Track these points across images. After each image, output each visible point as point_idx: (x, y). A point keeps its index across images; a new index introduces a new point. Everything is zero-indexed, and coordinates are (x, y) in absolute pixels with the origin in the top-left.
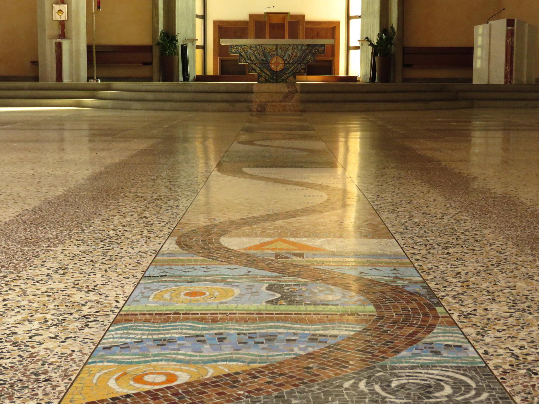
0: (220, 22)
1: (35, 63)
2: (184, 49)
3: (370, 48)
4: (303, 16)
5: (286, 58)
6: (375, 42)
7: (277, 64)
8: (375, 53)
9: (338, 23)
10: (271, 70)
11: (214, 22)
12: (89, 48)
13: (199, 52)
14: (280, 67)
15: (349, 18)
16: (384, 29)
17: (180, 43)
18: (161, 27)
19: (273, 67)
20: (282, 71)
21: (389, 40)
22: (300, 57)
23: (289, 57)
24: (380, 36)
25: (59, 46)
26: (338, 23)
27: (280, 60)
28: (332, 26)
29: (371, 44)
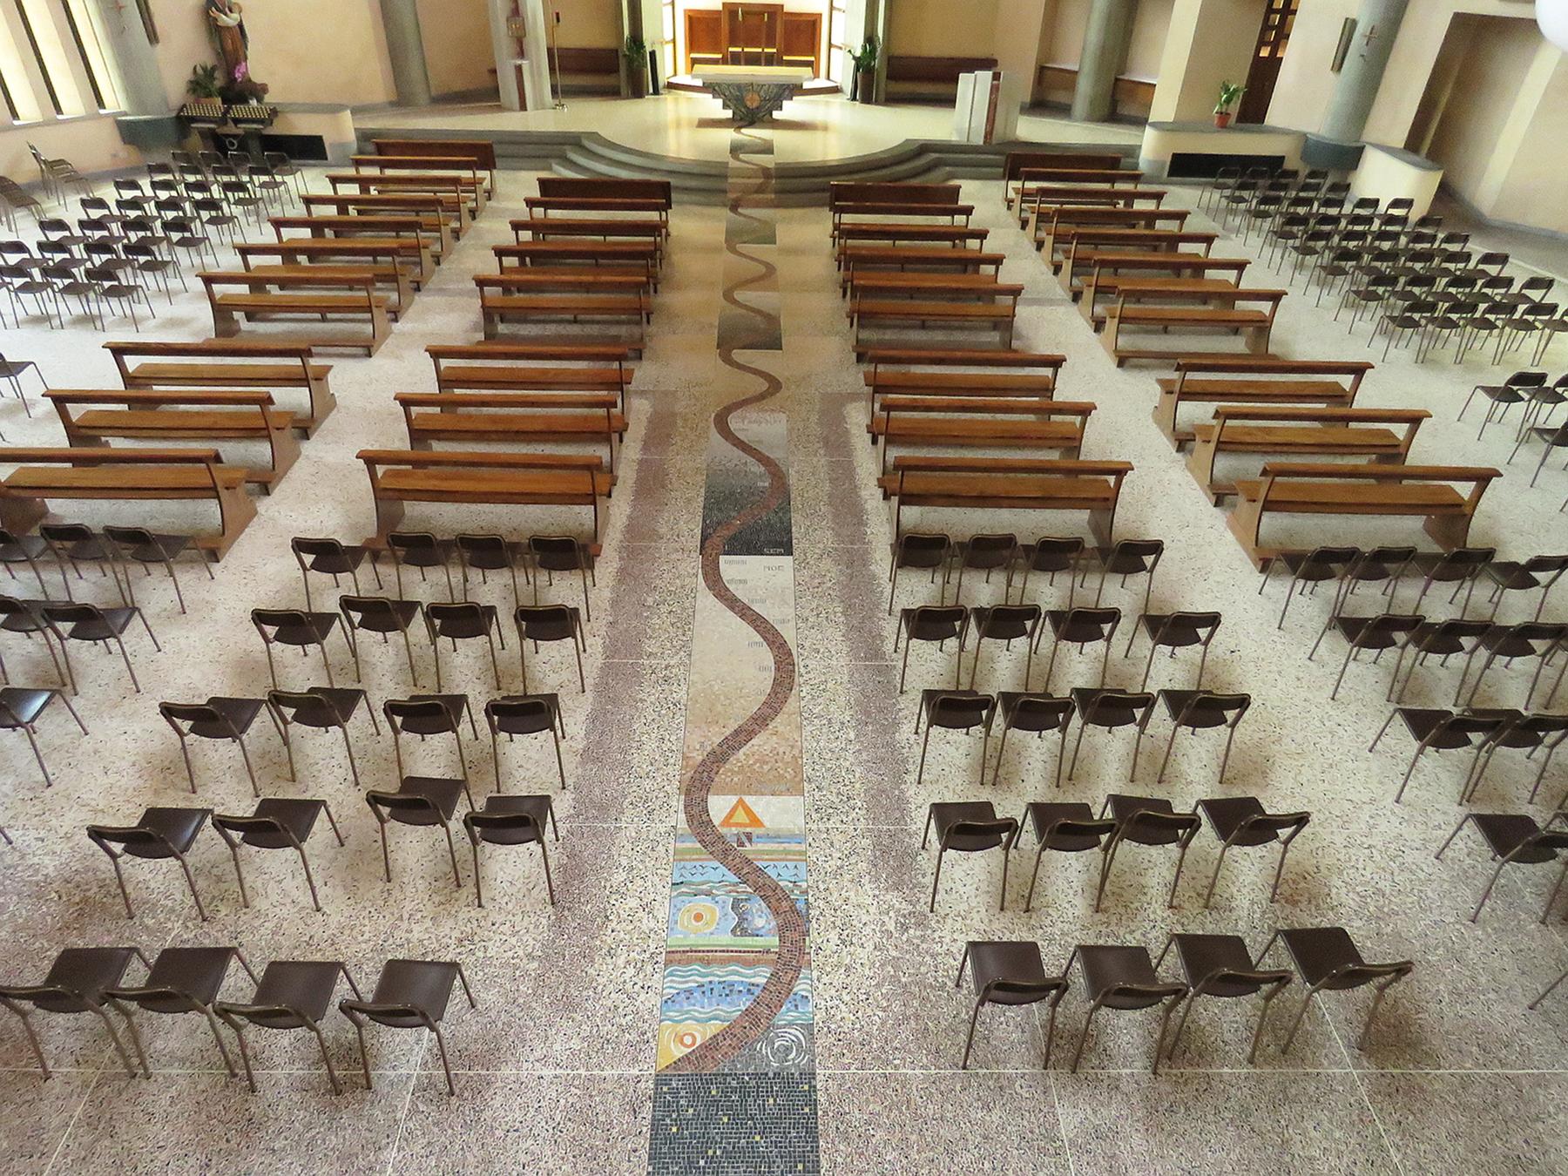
0: (690, 11)
1: (494, 72)
2: (653, 54)
3: (853, 62)
4: (782, 6)
5: (762, 93)
6: (858, 53)
7: (752, 100)
8: (857, 69)
9: (820, 15)
10: (746, 106)
11: (685, 11)
12: (550, 51)
13: (669, 48)
14: (755, 105)
15: (832, 8)
16: (870, 39)
17: (648, 49)
18: (626, 32)
19: (749, 104)
20: (757, 108)
21: (873, 50)
22: (777, 93)
23: (766, 94)
24: (864, 47)
25: (519, 69)
26: (820, 15)
27: (757, 97)
28: (813, 19)
29: (854, 58)
